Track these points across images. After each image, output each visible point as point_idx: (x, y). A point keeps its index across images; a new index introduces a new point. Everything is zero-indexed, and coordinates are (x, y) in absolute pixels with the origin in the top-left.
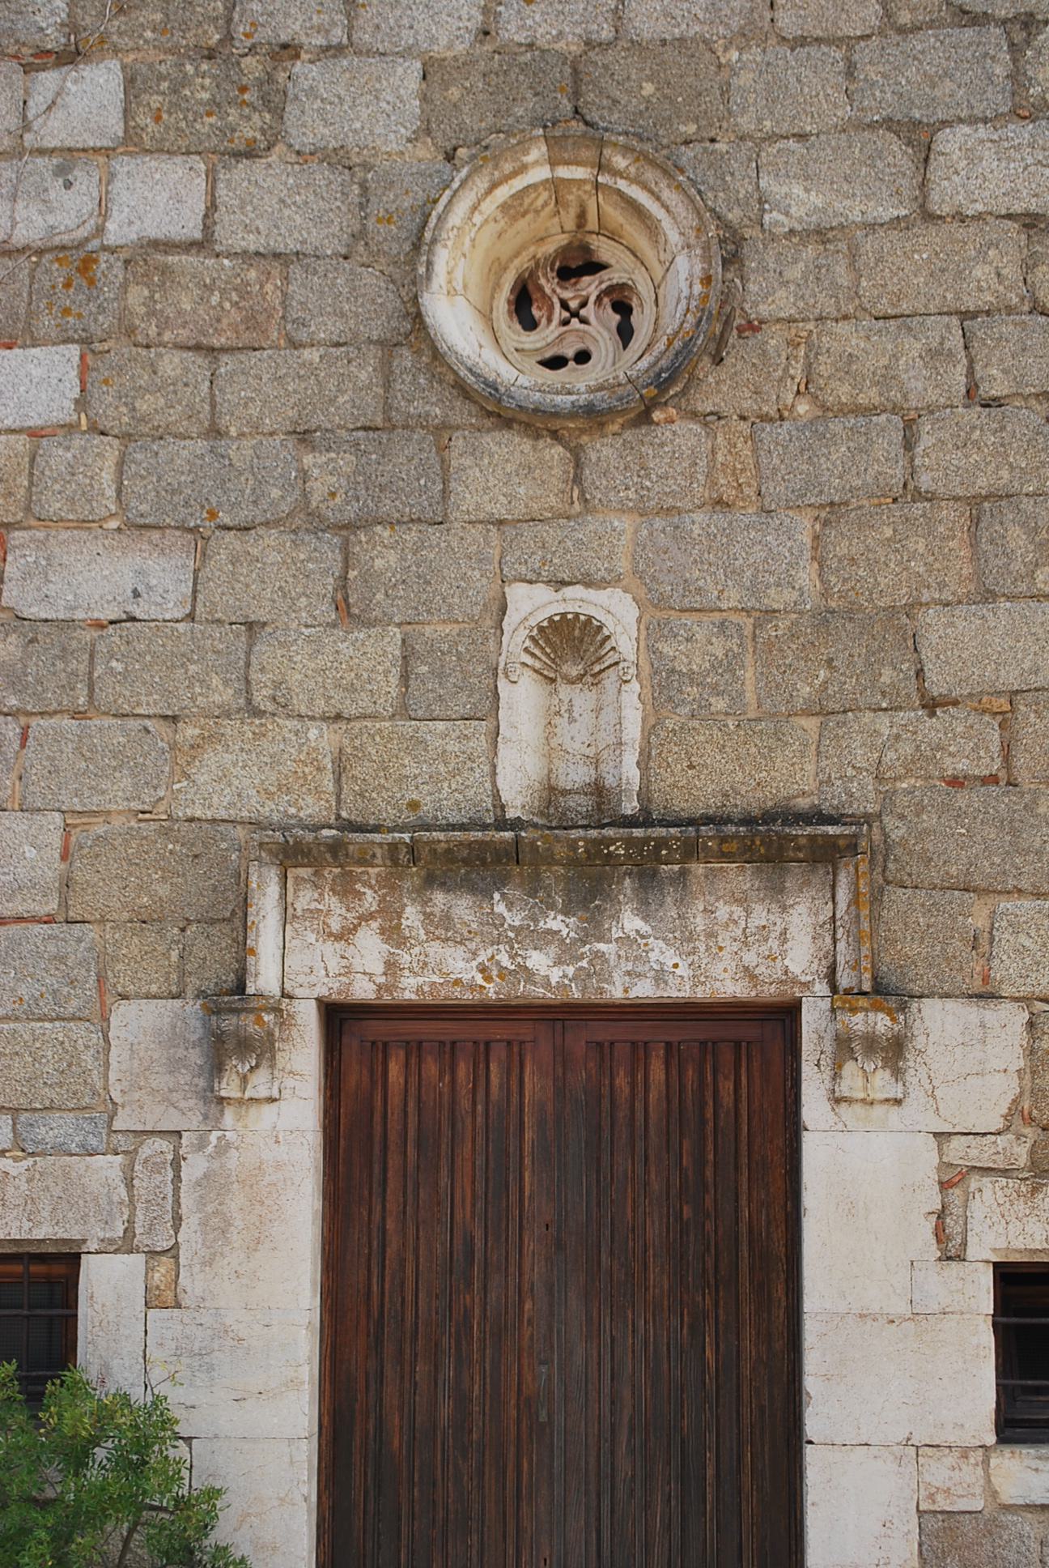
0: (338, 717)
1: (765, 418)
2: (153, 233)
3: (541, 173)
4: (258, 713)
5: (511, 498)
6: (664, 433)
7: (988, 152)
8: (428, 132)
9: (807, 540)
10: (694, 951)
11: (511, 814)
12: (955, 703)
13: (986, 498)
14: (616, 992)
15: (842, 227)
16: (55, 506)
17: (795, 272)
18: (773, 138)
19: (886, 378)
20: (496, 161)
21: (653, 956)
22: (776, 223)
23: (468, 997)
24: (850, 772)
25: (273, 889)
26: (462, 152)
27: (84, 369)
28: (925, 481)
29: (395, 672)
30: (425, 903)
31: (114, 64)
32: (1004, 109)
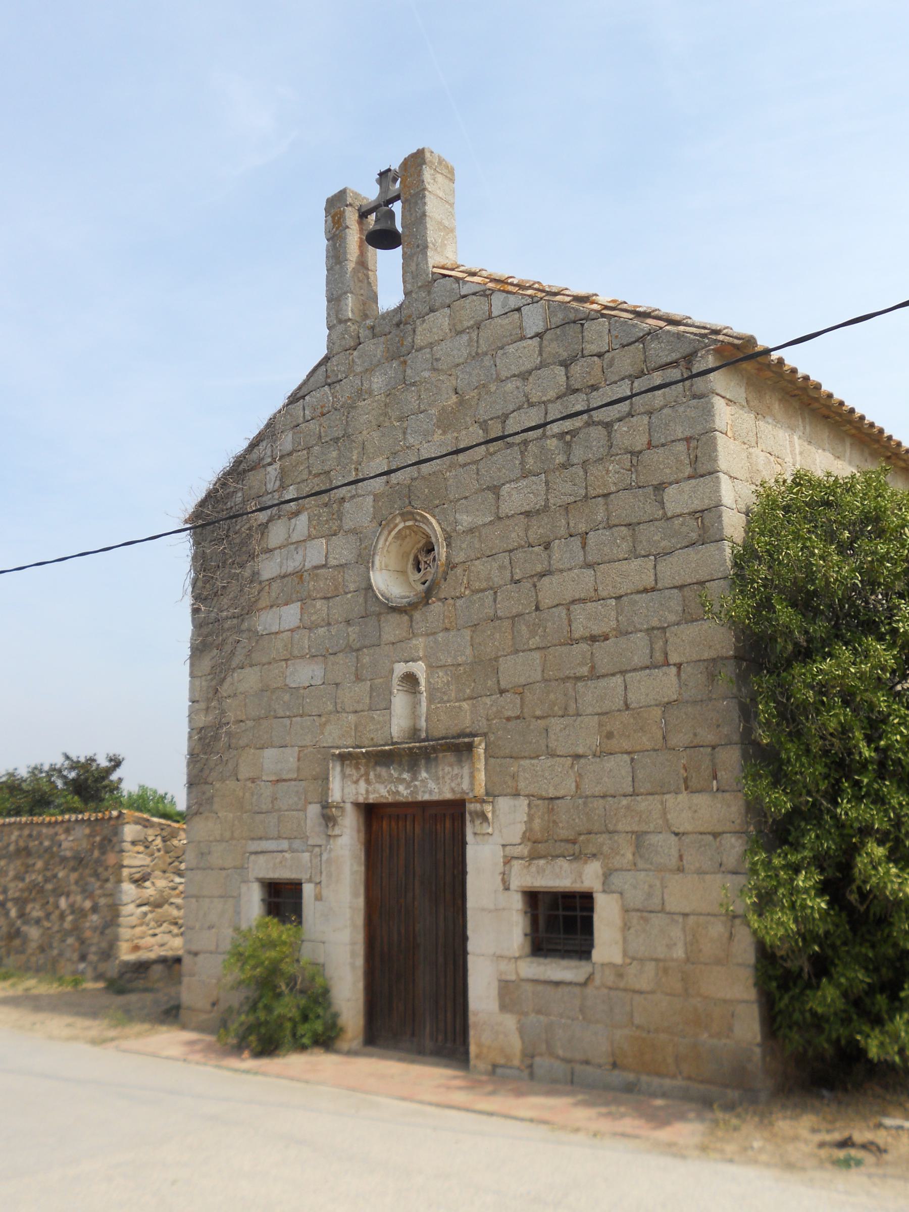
0: (356, 712)
1: (458, 598)
2: (315, 564)
3: (401, 526)
4: (338, 712)
5: (395, 635)
6: (432, 607)
7: (514, 493)
8: (375, 518)
9: (469, 638)
10: (439, 784)
11: (395, 740)
12: (508, 691)
13: (516, 616)
14: (420, 798)
15: (476, 527)
16: (296, 653)
17: (464, 546)
18: (459, 500)
19: (489, 579)
20: (388, 524)
21: (429, 785)
22: (459, 530)
23: (384, 801)
24: (480, 718)
25: (338, 769)
26: (383, 523)
27: (302, 608)
28: (500, 613)
29: (368, 695)
30: (375, 770)
31: (306, 513)
32: (519, 476)
